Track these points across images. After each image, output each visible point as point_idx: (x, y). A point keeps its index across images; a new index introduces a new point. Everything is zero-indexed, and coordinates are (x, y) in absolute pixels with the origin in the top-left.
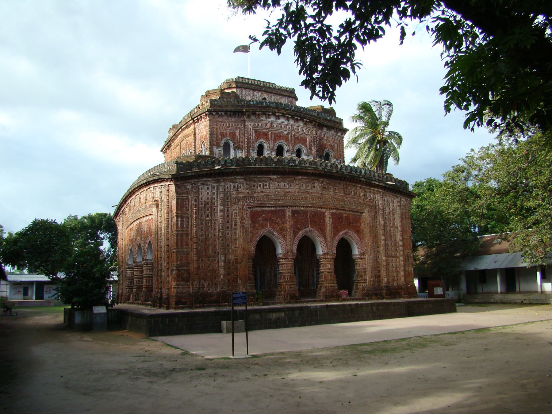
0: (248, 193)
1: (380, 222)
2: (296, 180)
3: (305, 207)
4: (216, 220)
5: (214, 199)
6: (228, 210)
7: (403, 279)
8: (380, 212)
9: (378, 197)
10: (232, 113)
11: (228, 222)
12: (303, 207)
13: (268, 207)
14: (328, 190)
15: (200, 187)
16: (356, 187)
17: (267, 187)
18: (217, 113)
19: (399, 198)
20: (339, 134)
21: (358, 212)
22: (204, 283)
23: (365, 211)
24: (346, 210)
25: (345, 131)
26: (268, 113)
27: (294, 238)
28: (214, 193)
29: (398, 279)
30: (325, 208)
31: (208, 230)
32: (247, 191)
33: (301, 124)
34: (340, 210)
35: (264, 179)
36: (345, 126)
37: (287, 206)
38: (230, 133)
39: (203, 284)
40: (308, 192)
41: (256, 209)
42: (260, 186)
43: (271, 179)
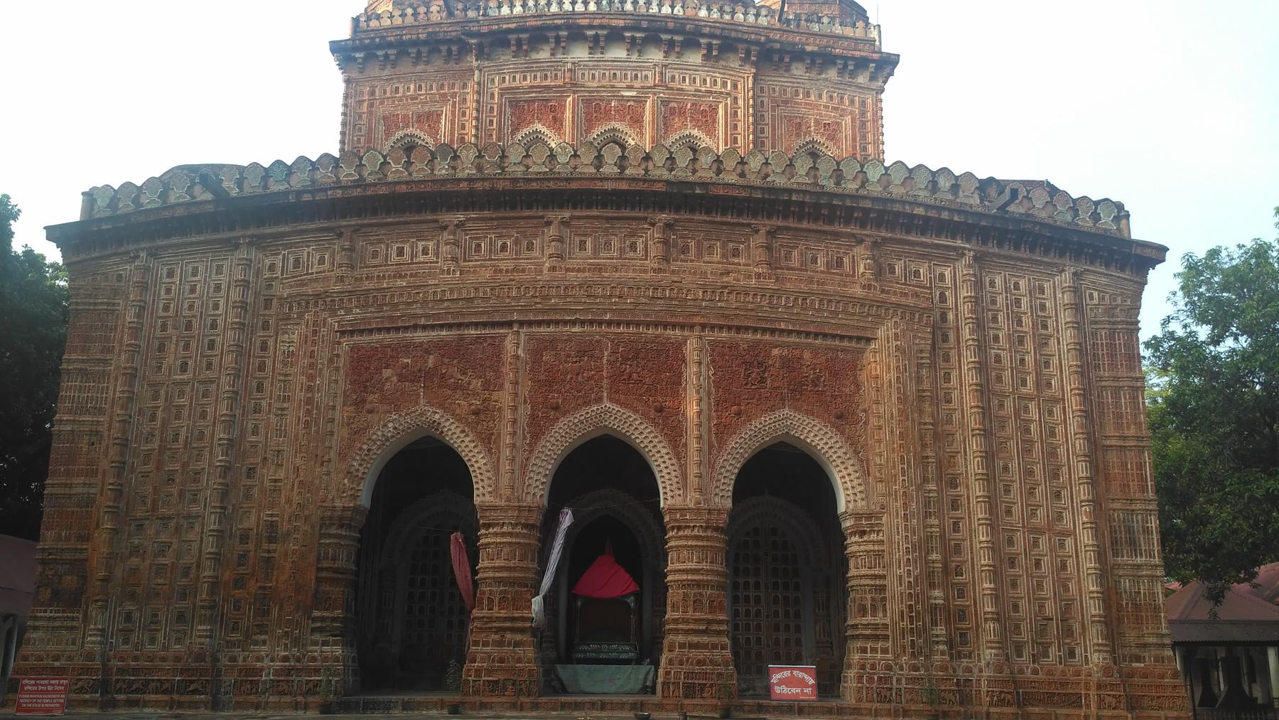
0: (341, 279)
1: (965, 376)
2: (549, 223)
3: (591, 322)
4: (212, 382)
5: (216, 306)
6: (264, 347)
7: (1095, 635)
8: (966, 333)
9: (955, 279)
10: (424, 49)
11: (260, 388)
12: (583, 323)
13: (424, 327)
14: (699, 255)
15: (165, 271)
16: (837, 235)
17: (431, 257)
18: (370, 57)
19: (1067, 275)
20: (862, 79)
21: (842, 338)
22: (136, 615)
23: (881, 333)
24: (782, 331)
25: (887, 64)
26: (553, 34)
27: (532, 446)
28: (218, 288)
29: (1069, 632)
30: (683, 327)
31: (178, 417)
32: (338, 272)
33: (695, 58)
34: (755, 330)
35: (413, 227)
36: (887, 47)
37: (509, 324)
38: (419, 117)
39: (128, 617)
40: (599, 269)
41: (376, 337)
42: (400, 252)
43: (445, 228)
